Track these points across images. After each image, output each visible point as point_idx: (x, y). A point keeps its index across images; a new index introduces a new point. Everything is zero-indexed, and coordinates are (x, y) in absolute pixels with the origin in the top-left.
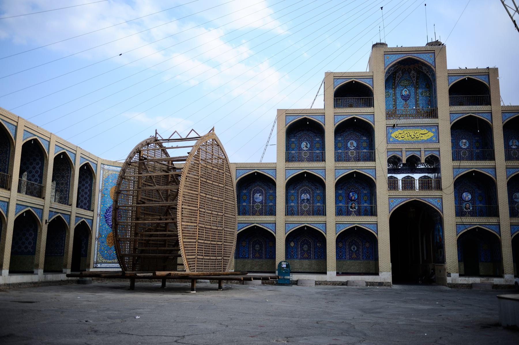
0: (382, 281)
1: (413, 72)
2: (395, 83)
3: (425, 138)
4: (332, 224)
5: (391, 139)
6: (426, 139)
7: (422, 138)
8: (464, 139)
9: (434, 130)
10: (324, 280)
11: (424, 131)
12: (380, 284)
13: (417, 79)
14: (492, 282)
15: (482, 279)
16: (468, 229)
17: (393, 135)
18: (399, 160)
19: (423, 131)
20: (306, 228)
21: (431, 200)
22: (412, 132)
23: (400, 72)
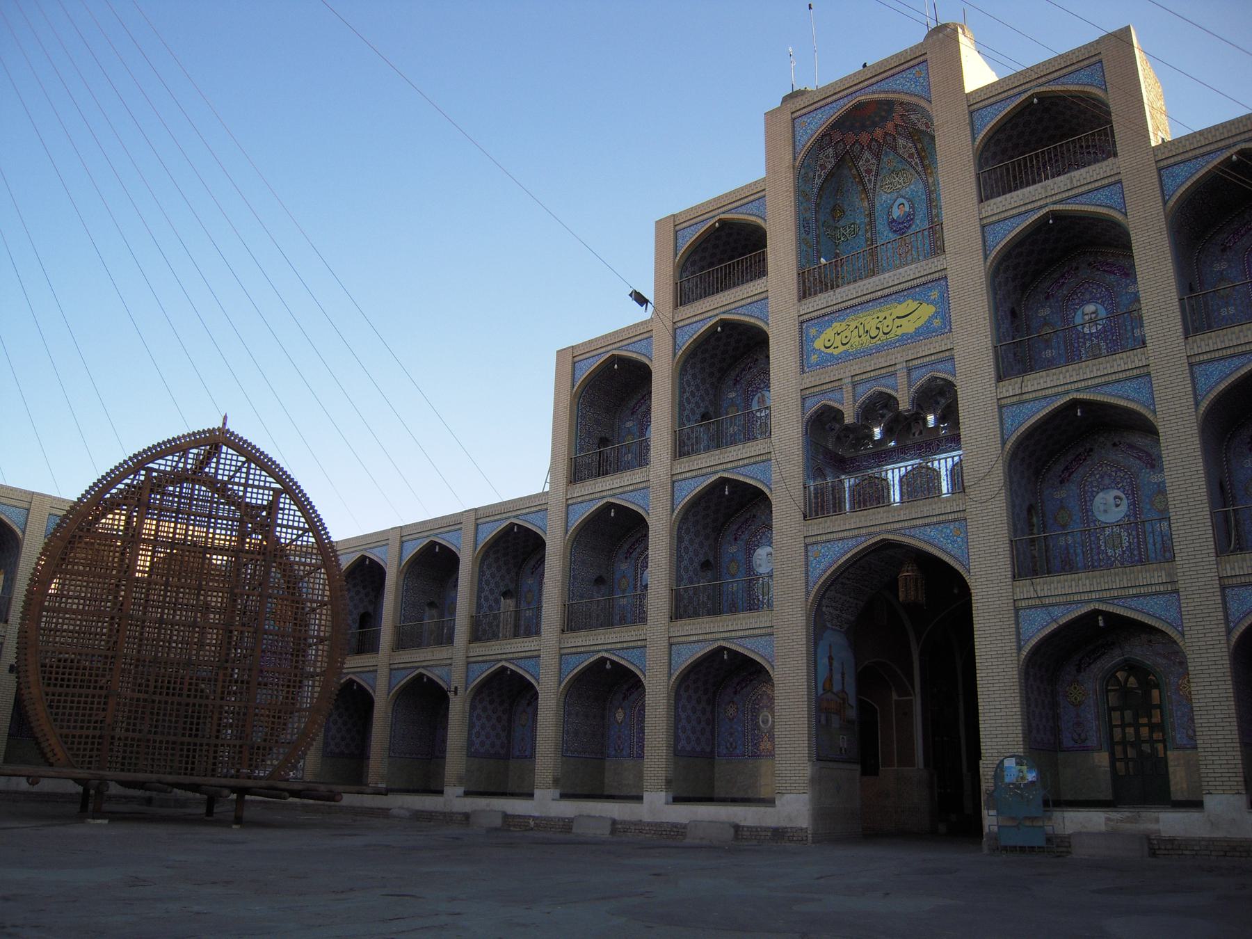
0: (783, 824)
1: (901, 142)
3: (909, 327)
4: (659, 645)
5: (814, 358)
6: (911, 330)
7: (900, 332)
8: (1089, 302)
9: (934, 295)
10: (635, 818)
12: (778, 833)
13: (922, 159)
14: (1153, 827)
15: (1115, 815)
16: (1062, 621)
17: (818, 344)
18: (837, 415)
19: (901, 309)
20: (608, 666)
21: (932, 533)
22: (870, 321)
23: (867, 154)
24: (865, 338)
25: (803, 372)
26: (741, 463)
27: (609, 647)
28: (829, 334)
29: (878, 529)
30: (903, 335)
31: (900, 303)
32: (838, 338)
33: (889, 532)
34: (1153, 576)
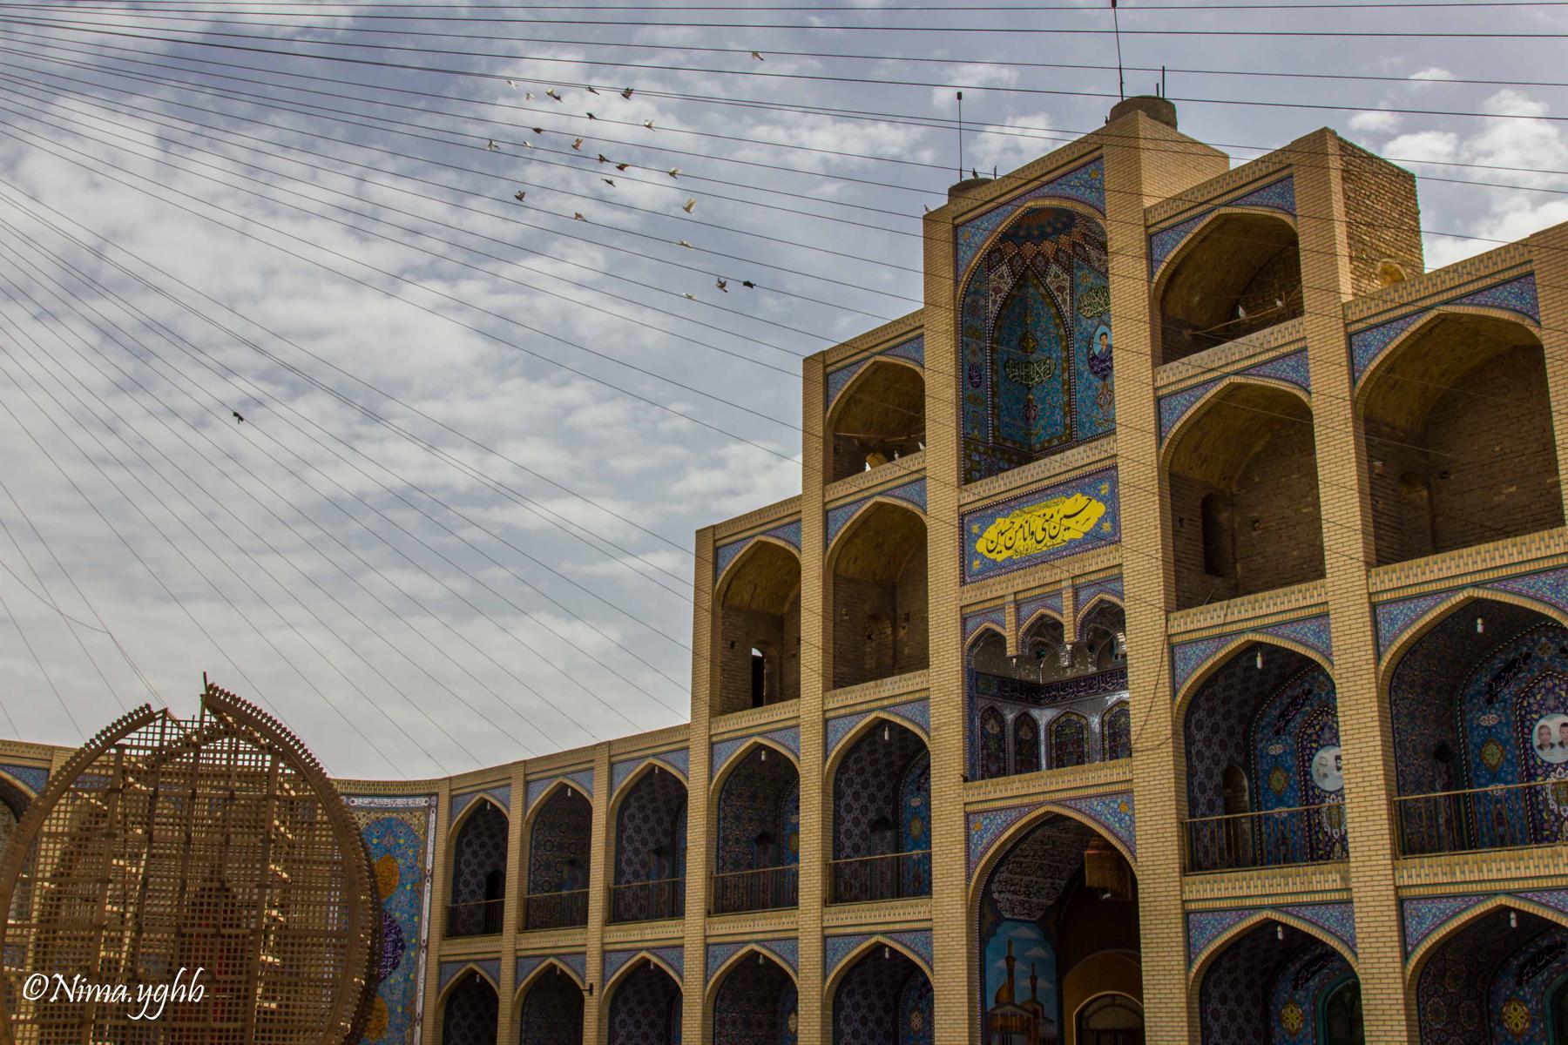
2: (1060, 314)
3: (1077, 529)
5: (976, 563)
6: (1080, 536)
7: (1068, 536)
9: (1105, 489)
11: (1078, 501)
17: (981, 546)
20: (761, 961)
23: (1054, 269)
24: (1031, 542)
25: (963, 583)
26: (898, 700)
27: (760, 937)
28: (991, 533)
29: (1041, 798)
30: (1070, 541)
31: (1068, 497)
32: (1002, 539)
33: (1053, 803)
34: (1321, 880)
